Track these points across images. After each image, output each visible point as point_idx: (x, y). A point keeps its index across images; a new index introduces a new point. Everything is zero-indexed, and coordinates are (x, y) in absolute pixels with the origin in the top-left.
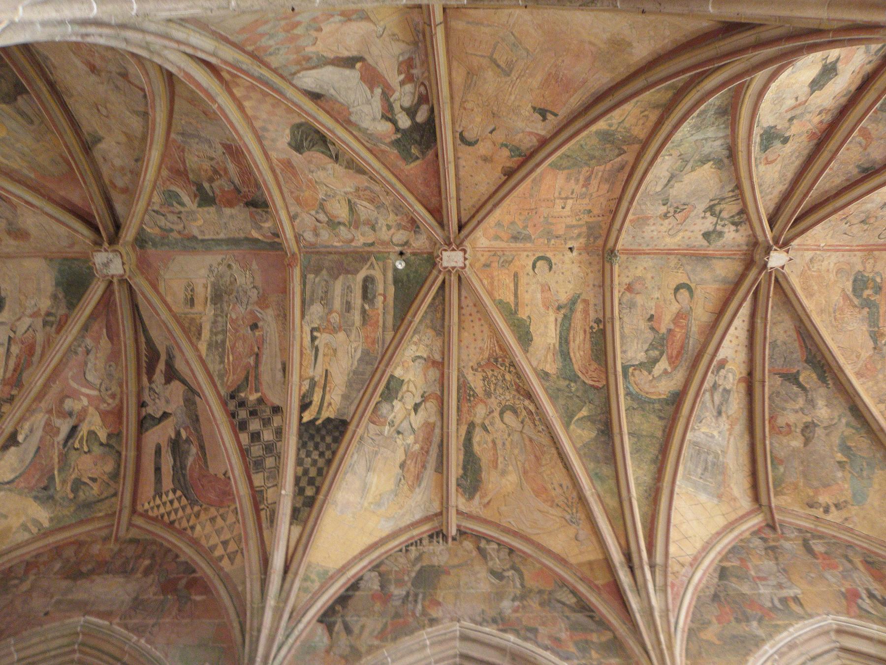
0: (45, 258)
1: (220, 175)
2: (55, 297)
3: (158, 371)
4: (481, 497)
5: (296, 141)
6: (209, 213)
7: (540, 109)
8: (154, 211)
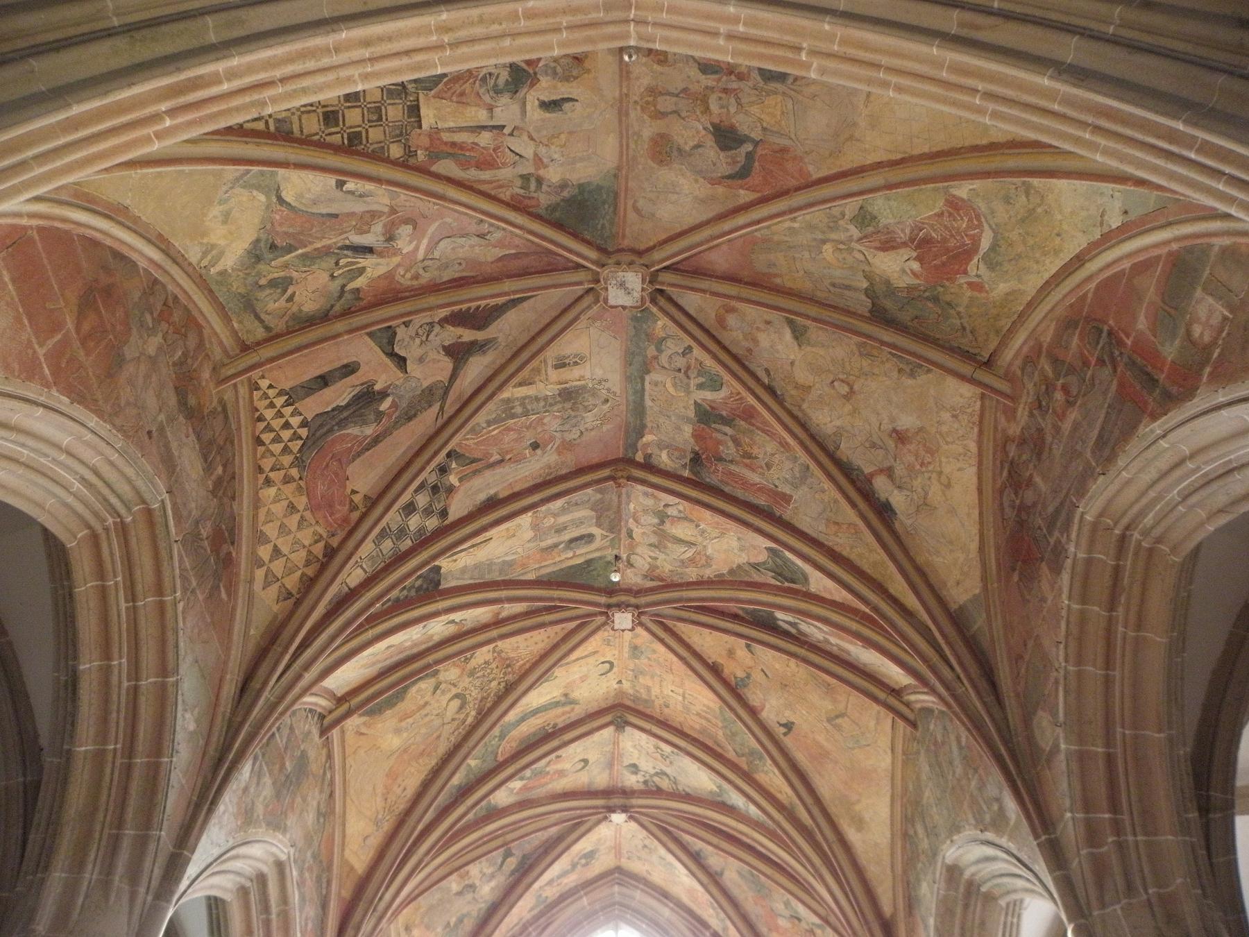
0: (619, 168)
2: (564, 185)
3: (460, 331)
4: (364, 723)
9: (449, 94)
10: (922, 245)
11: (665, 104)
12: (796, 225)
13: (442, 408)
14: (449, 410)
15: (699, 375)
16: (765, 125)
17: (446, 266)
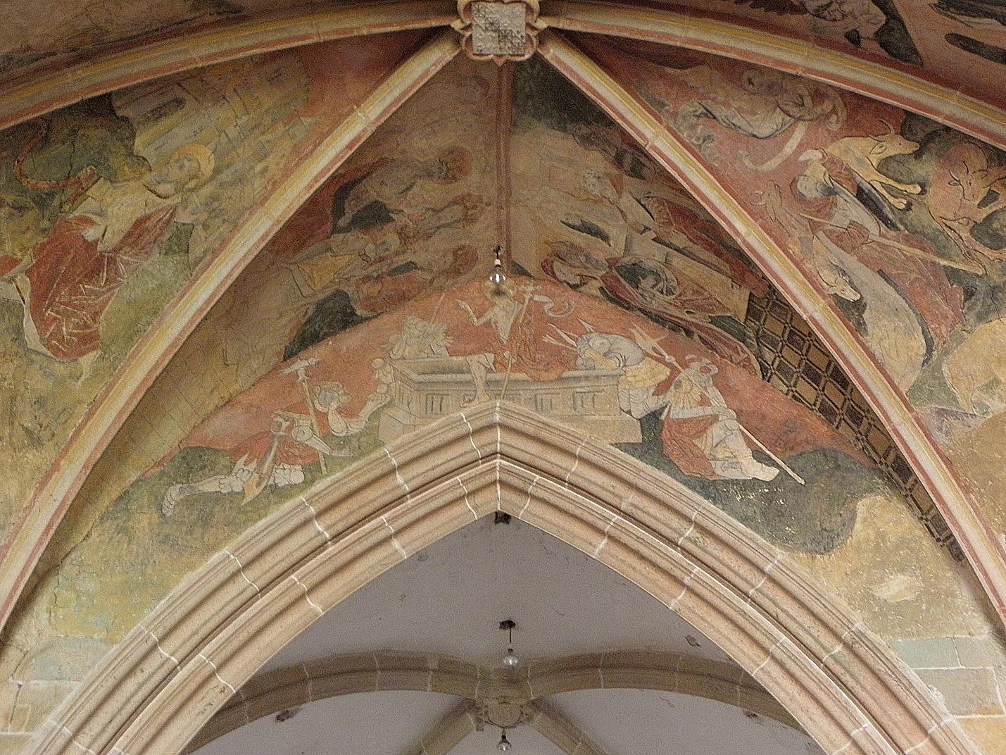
0: (510, 133)
2: (586, 140)
9: (710, 301)
10: (97, 264)
12: (259, 168)
16: (329, 254)
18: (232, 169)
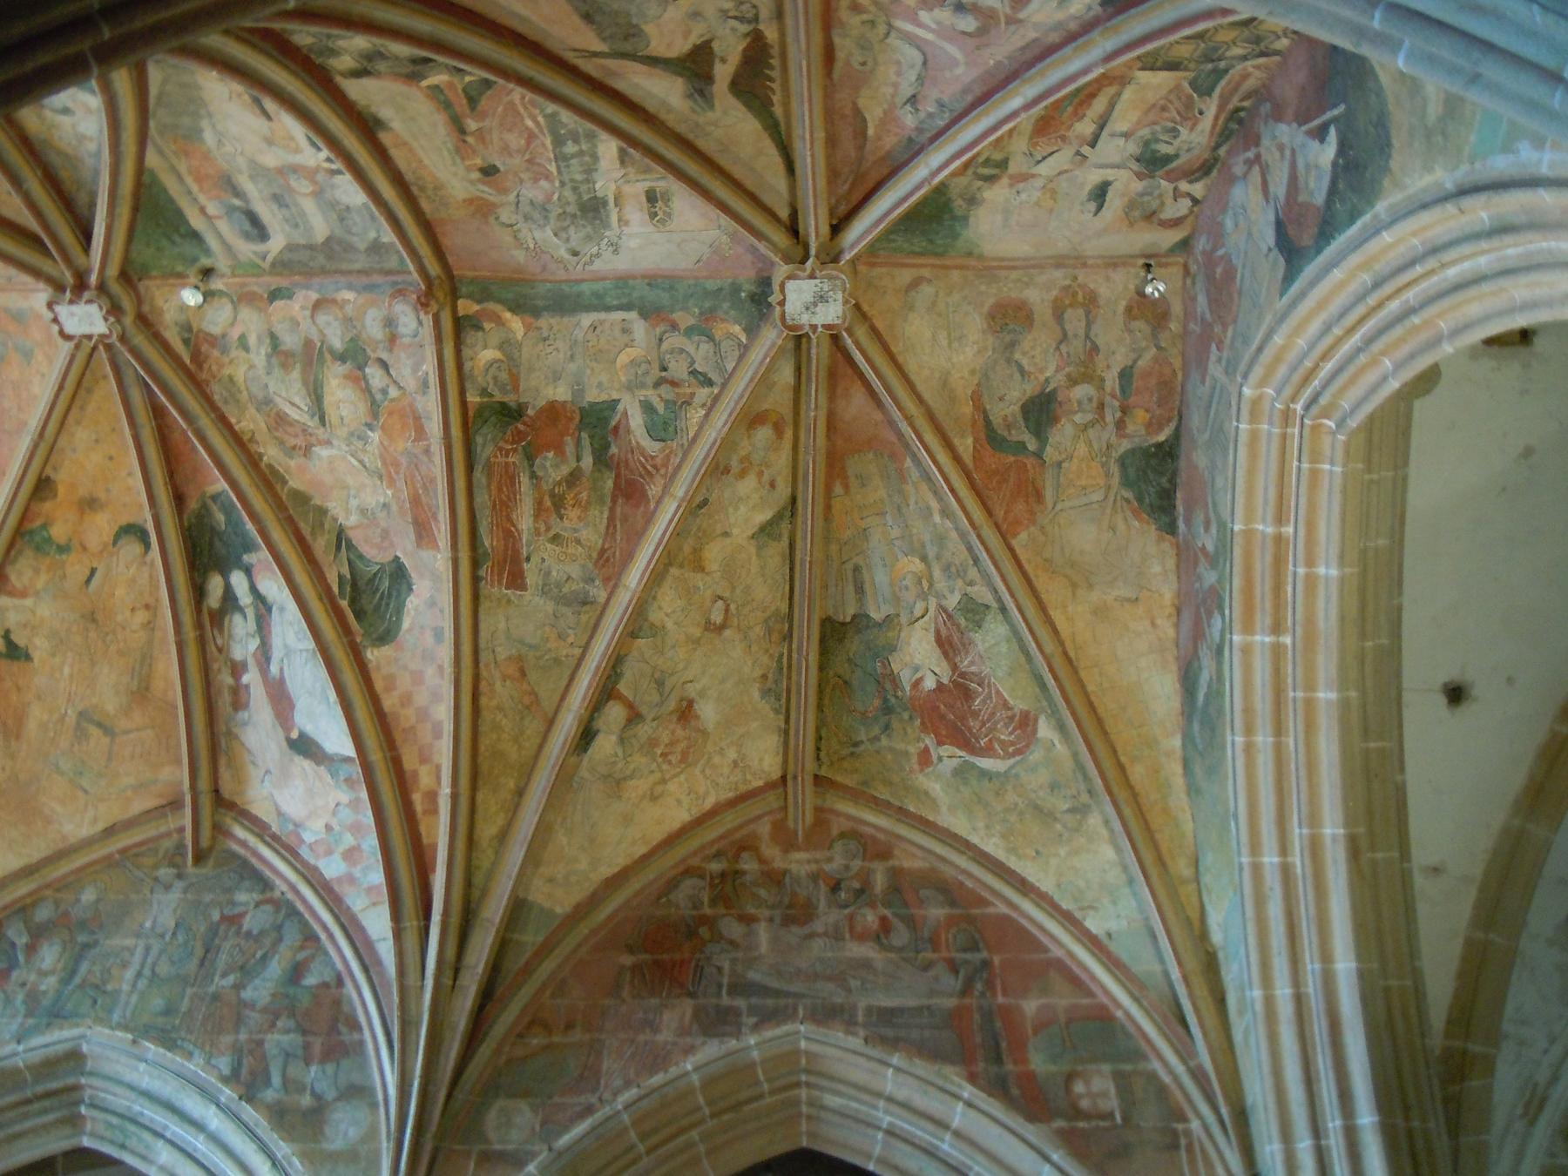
0: (981, 257)
1: (552, 495)
2: (972, 201)
5: (399, 591)
6: (600, 385)
7: (18, 658)
8: (710, 383)
10: (961, 689)
11: (1075, 320)
12: (937, 518)
13: (595, 54)
14: (588, 66)
15: (667, 402)
17: (865, 45)
18: (929, 546)
